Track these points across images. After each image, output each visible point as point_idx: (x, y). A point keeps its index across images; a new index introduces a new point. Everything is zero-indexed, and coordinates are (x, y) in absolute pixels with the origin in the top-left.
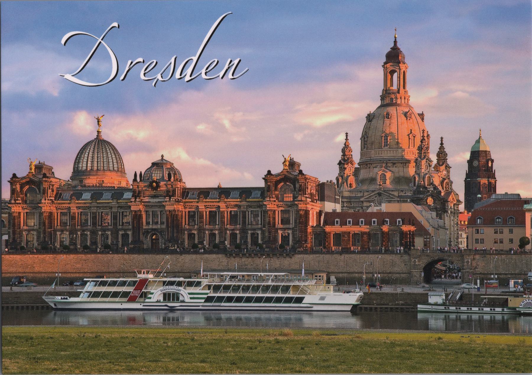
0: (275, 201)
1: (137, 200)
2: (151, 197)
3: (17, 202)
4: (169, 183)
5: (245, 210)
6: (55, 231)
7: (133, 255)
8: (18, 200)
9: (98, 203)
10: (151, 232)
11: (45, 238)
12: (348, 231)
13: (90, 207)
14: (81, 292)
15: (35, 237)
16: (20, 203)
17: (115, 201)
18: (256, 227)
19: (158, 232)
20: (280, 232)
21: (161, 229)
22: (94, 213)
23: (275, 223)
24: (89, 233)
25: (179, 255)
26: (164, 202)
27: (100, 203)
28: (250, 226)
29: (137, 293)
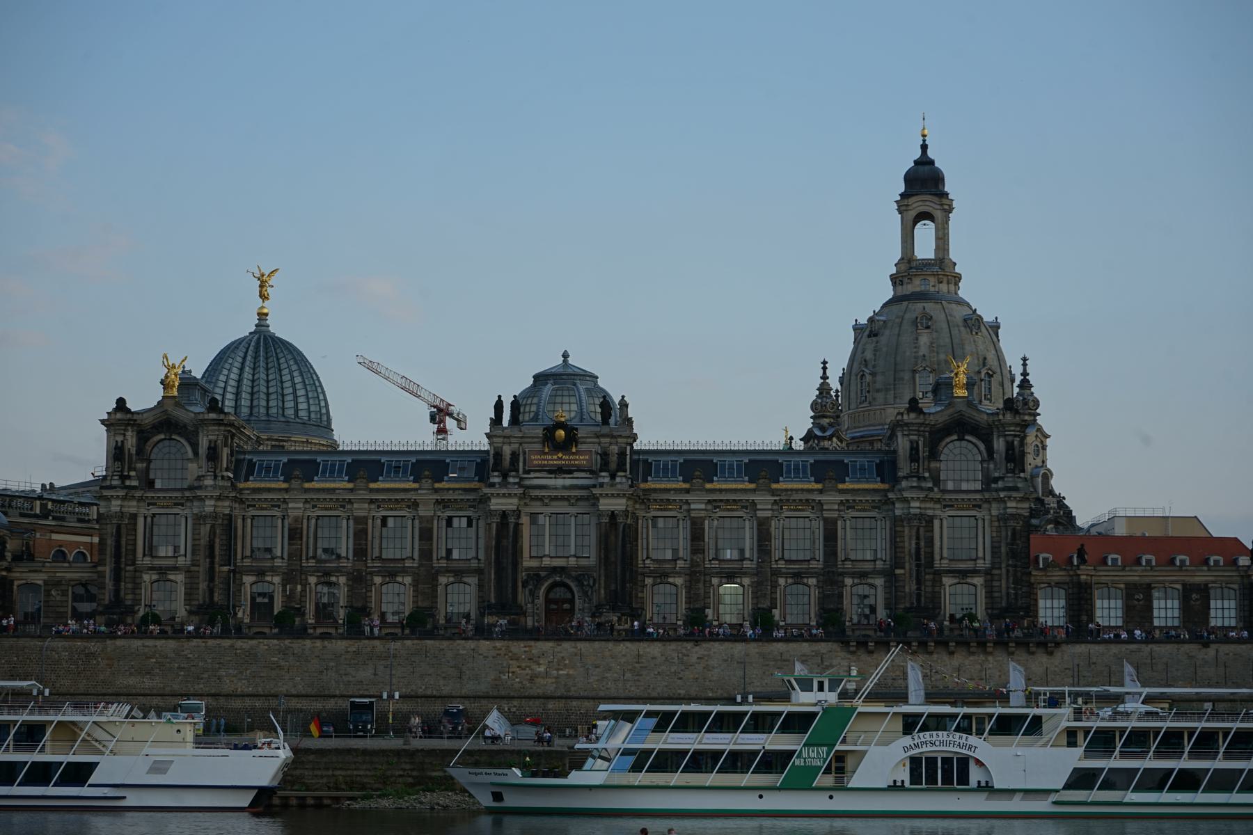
0: (931, 489)
1: (511, 480)
2: (550, 472)
3: (128, 483)
4: (605, 430)
5: (835, 515)
6: (237, 572)
7: (540, 644)
8: (129, 477)
9: (371, 490)
10: (548, 577)
11: (211, 592)
12: (1147, 580)
13: (350, 502)
14: (587, 754)
15: (181, 590)
16: (134, 488)
17: (427, 483)
18: (868, 567)
19: (569, 576)
20: (947, 581)
21: (579, 568)
22: (358, 520)
23: (932, 553)
24: (342, 580)
25: (689, 645)
26: (594, 486)
27: (378, 491)
28: (848, 565)
29: (817, 757)
